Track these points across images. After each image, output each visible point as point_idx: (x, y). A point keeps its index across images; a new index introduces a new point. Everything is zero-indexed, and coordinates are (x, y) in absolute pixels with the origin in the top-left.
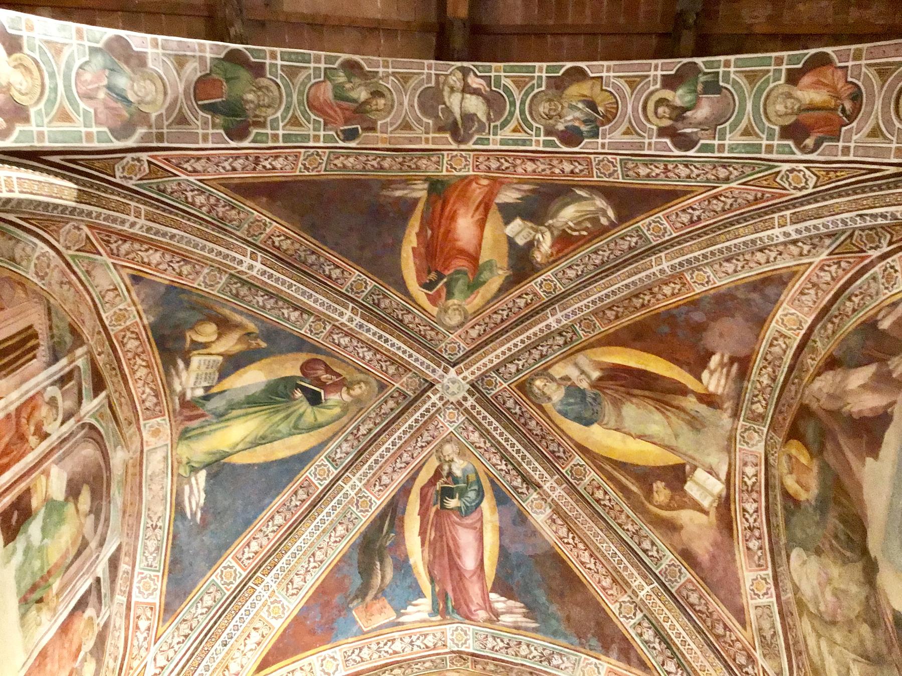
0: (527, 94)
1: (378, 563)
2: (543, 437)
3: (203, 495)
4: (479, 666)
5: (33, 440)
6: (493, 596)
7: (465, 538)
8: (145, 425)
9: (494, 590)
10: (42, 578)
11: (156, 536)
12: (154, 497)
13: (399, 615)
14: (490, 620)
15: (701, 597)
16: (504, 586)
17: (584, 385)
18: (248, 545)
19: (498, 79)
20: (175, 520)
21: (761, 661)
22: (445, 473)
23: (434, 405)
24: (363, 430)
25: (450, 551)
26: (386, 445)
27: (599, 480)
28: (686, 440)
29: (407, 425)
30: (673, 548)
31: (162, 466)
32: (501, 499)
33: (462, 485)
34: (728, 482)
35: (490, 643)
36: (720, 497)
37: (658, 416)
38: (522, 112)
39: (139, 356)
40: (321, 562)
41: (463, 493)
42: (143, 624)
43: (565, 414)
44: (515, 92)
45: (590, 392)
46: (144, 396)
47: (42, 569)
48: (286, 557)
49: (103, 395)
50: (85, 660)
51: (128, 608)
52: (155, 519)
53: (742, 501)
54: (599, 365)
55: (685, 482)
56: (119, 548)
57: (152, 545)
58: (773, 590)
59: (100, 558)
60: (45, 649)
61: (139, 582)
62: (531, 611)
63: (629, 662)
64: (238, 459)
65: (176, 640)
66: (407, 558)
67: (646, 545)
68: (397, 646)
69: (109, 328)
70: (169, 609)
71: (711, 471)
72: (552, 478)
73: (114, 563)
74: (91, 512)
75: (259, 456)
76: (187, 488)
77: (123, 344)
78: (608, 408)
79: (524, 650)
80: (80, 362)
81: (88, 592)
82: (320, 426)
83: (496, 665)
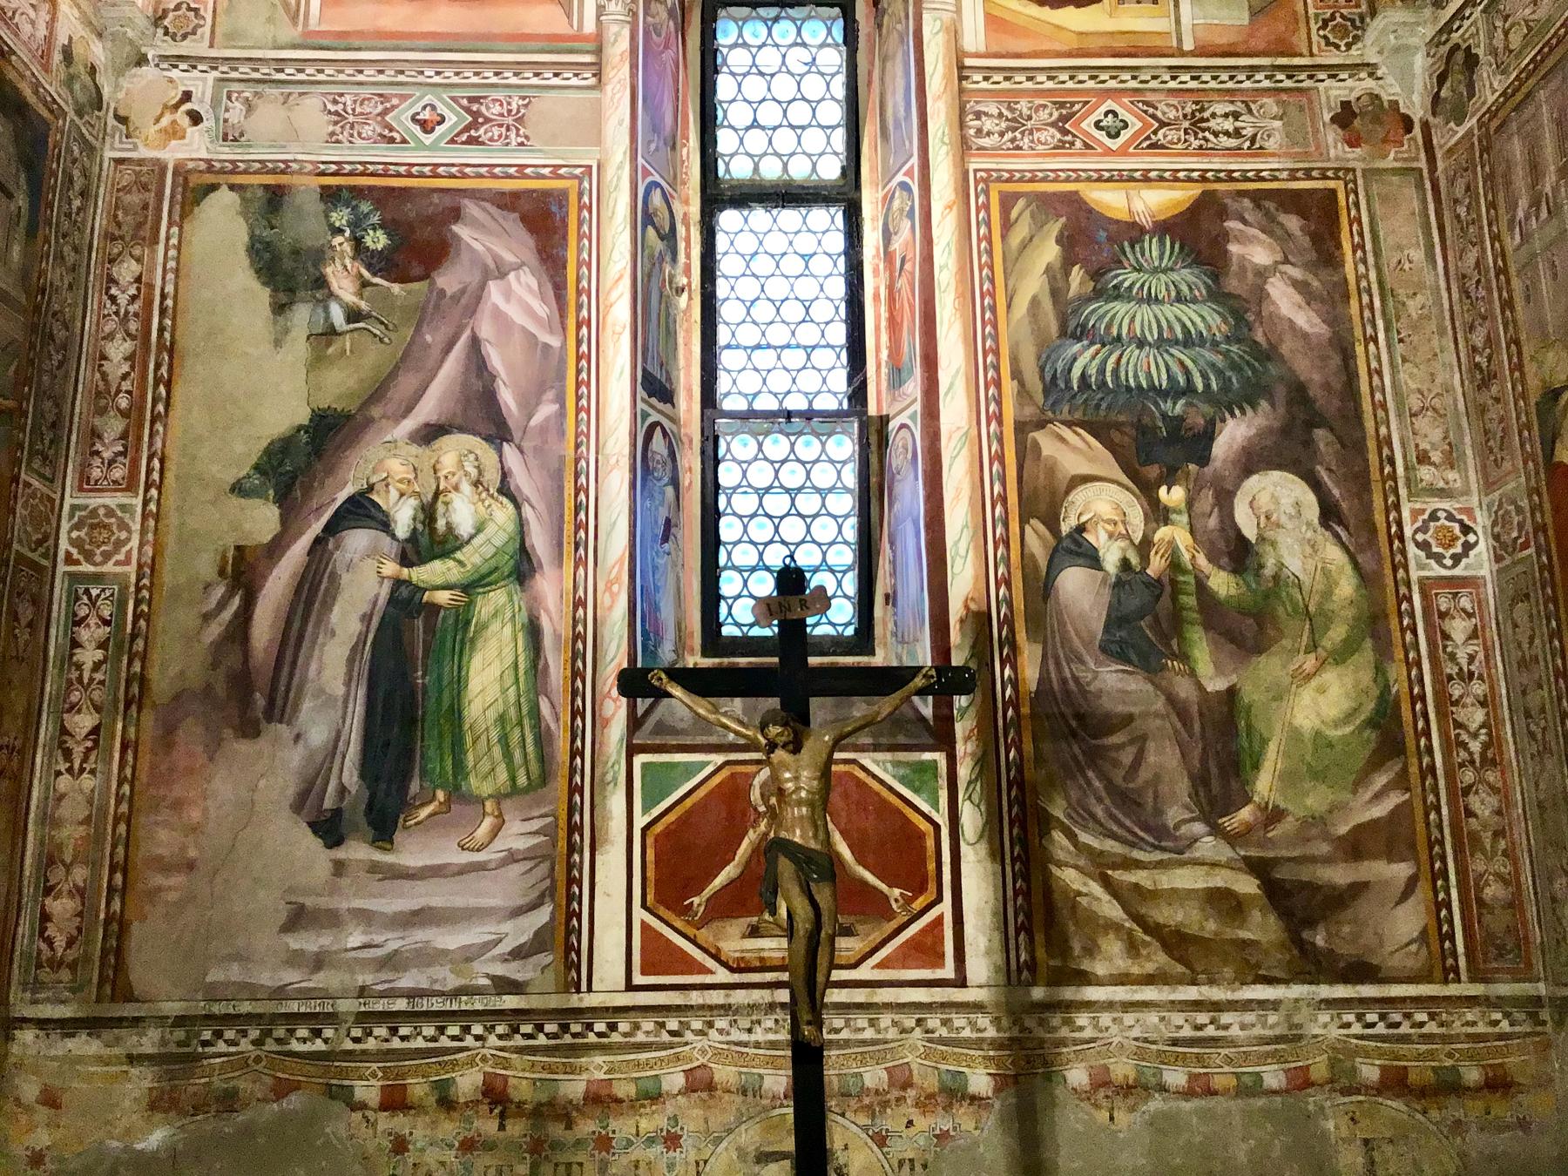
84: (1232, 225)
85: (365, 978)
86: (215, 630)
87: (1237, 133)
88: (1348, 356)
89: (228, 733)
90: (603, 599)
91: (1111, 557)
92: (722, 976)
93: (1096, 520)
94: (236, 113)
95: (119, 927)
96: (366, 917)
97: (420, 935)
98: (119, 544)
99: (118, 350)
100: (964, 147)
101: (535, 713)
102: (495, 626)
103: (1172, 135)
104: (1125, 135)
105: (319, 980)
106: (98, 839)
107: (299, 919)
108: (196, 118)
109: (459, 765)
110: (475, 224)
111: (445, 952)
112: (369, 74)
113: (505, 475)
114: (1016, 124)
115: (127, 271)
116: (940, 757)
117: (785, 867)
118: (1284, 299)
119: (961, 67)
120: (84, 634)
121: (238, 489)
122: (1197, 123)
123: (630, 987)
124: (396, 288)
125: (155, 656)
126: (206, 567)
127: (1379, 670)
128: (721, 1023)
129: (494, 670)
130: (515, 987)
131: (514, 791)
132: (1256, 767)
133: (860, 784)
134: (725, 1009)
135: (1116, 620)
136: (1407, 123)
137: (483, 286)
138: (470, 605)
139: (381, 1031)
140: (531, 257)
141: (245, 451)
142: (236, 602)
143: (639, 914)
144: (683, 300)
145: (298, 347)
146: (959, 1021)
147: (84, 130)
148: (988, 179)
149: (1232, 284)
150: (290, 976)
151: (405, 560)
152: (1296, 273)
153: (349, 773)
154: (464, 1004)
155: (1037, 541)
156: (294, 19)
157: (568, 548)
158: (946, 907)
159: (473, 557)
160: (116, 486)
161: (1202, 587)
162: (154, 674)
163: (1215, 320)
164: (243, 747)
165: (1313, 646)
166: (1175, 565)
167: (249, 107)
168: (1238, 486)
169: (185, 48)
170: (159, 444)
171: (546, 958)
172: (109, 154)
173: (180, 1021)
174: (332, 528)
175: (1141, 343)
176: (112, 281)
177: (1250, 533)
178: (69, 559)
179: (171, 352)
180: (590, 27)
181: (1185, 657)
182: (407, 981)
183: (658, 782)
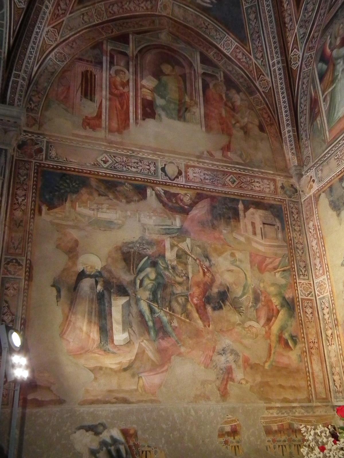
5: (126, 90)
8: (159, 12)
10: (179, 105)
11: (211, 29)
12: (194, 22)
20: (209, 15)
31: (182, 11)
39: (123, 5)
42: (240, 56)
46: (145, 8)
47: (175, 103)
49: (131, 36)
50: (227, 95)
52: (203, 25)
56: (201, 54)
57: (213, 33)
59: (196, 68)
60: (205, 113)
61: (224, 48)
65: (257, 43)
69: (104, 20)
70: (243, 40)
73: (205, 60)
74: (173, 67)
77: (114, 14)
80: (109, 48)
81: (204, 81)
115: (311, 224)
147: (293, 200)
170: (326, 262)
176: (309, 228)
179: (322, 238)
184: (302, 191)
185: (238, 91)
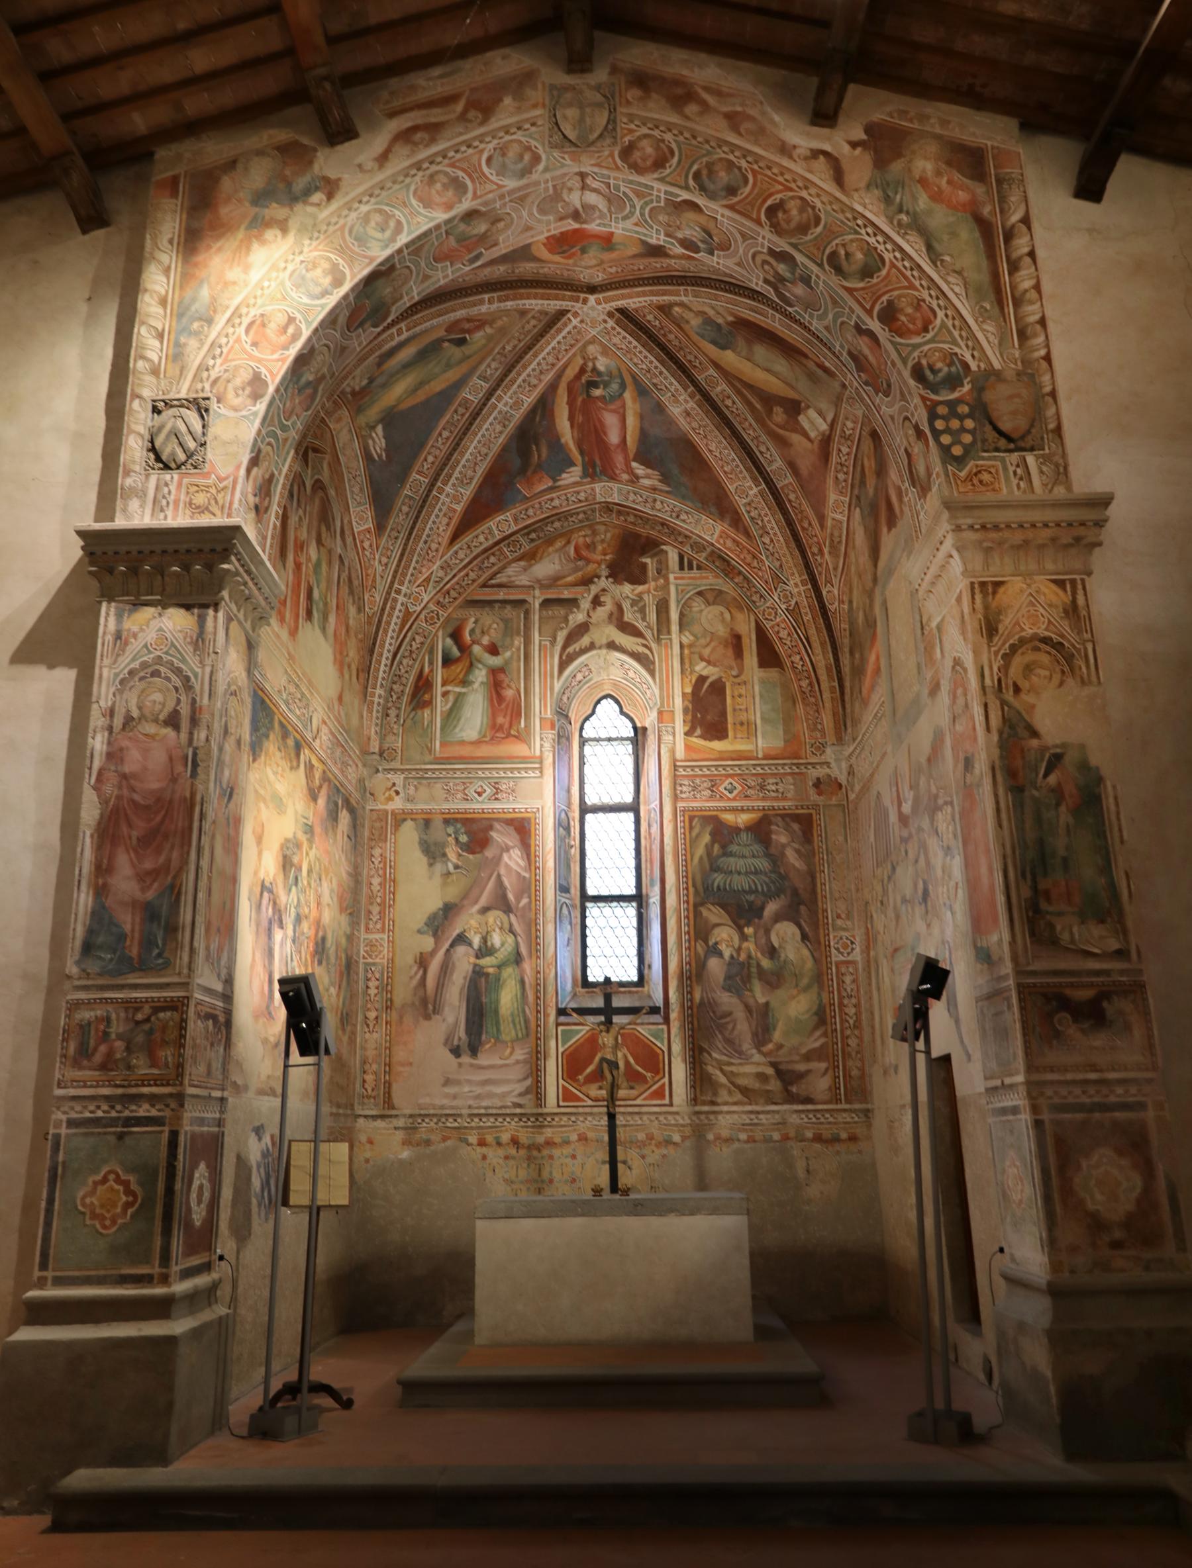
0: (646, 204)
1: (534, 447)
2: (681, 348)
3: (383, 441)
4: (622, 518)
6: (634, 464)
7: (610, 420)
9: (635, 460)
13: (555, 481)
14: (632, 482)
15: (797, 498)
16: (643, 457)
17: (720, 321)
18: (426, 460)
19: (617, 188)
21: (827, 556)
22: (589, 369)
23: (575, 327)
24: (508, 348)
25: (596, 430)
26: (532, 366)
27: (729, 391)
28: (803, 385)
29: (550, 347)
30: (783, 457)
32: (642, 391)
33: (606, 378)
34: (832, 426)
35: (632, 497)
36: (823, 434)
37: (783, 361)
38: (642, 214)
40: (486, 455)
41: (606, 385)
42: (366, 544)
43: (702, 336)
44: (635, 200)
45: (726, 328)
48: (458, 469)
51: (354, 539)
53: (839, 443)
54: (732, 314)
55: (799, 414)
57: (356, 490)
58: (846, 512)
62: (666, 478)
63: (737, 530)
64: (404, 406)
66: (558, 439)
67: (763, 449)
68: (556, 503)
70: (380, 527)
71: (820, 414)
72: (686, 390)
75: (421, 396)
76: (370, 442)
78: (741, 343)
79: (658, 505)
82: (469, 357)
83: (636, 516)
84: (773, 827)
85: (471, 1102)
86: (415, 982)
87: (777, 791)
88: (813, 878)
89: (421, 1019)
90: (547, 971)
91: (727, 954)
92: (590, 1103)
93: (722, 939)
94: (412, 790)
95: (388, 1085)
96: (469, 1082)
97: (488, 1088)
98: (380, 952)
99: (376, 881)
100: (675, 798)
101: (524, 1011)
102: (508, 981)
103: (752, 792)
104: (735, 792)
105: (455, 1103)
106: (380, 1055)
107: (447, 1082)
108: (397, 793)
109: (498, 1030)
110: (498, 831)
111: (496, 1095)
112: (458, 774)
113: (511, 925)
114: (695, 788)
115: (377, 852)
116: (665, 1027)
117: (605, 1065)
118: (791, 856)
119: (675, 766)
120: (371, 984)
121: (419, 931)
122: (762, 787)
123: (559, 1106)
124: (471, 856)
125: (395, 993)
126: (410, 959)
127: (819, 994)
128: (590, 1118)
129: (509, 997)
130: (520, 1106)
131: (517, 1039)
132: (774, 1029)
133: (637, 1037)
134: (591, 1114)
135: (728, 977)
136: (840, 786)
137: (501, 855)
138: (500, 973)
139: (476, 1120)
140: (518, 843)
141: (419, 918)
142: (421, 972)
143: (561, 1081)
144: (573, 850)
145: (437, 880)
146: (670, 1117)
148: (684, 811)
149: (773, 851)
150: (445, 1102)
151: (477, 957)
152: (796, 846)
153: (462, 1032)
154: (503, 1111)
155: (700, 948)
156: (430, 751)
157: (534, 952)
158: (666, 1080)
159: (501, 955)
160: (378, 931)
161: (759, 965)
162: (395, 998)
163: (766, 864)
164: (426, 1023)
165: (797, 985)
166: (749, 957)
167: (416, 788)
168: (772, 926)
169: (393, 765)
171: (529, 1096)
172: (368, 807)
173: (411, 1116)
174: (452, 945)
175: (739, 873)
177: (776, 945)
178: (364, 958)
180: (538, 753)
181: (751, 990)
182: (484, 1104)
183: (567, 1036)
184: (372, 794)
185: (354, 602)
